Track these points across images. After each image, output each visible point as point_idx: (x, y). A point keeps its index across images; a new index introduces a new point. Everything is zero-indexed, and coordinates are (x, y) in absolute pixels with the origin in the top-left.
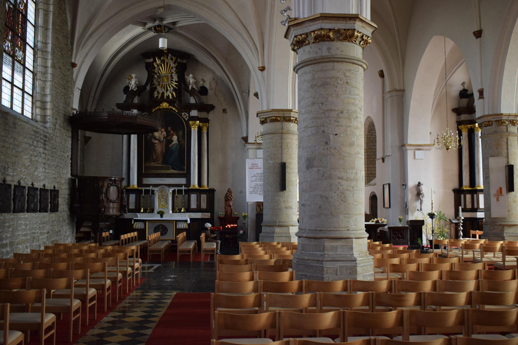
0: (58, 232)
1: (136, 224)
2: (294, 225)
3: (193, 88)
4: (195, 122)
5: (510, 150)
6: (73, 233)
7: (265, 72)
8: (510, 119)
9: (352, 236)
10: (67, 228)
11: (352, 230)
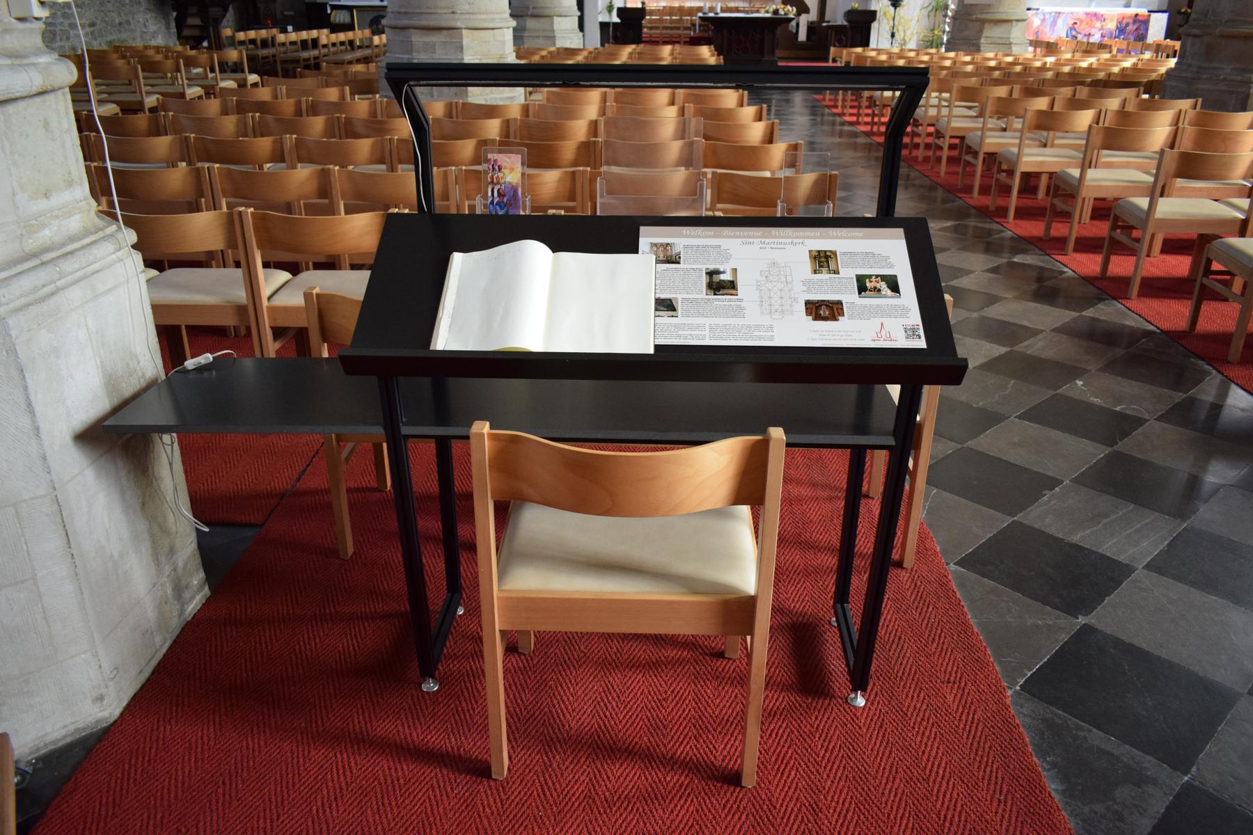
0: (120, 24)
1: (336, 14)
2: (565, 14)
6: (168, 28)
9: (459, 24)
10: (148, 16)
11: (462, 14)
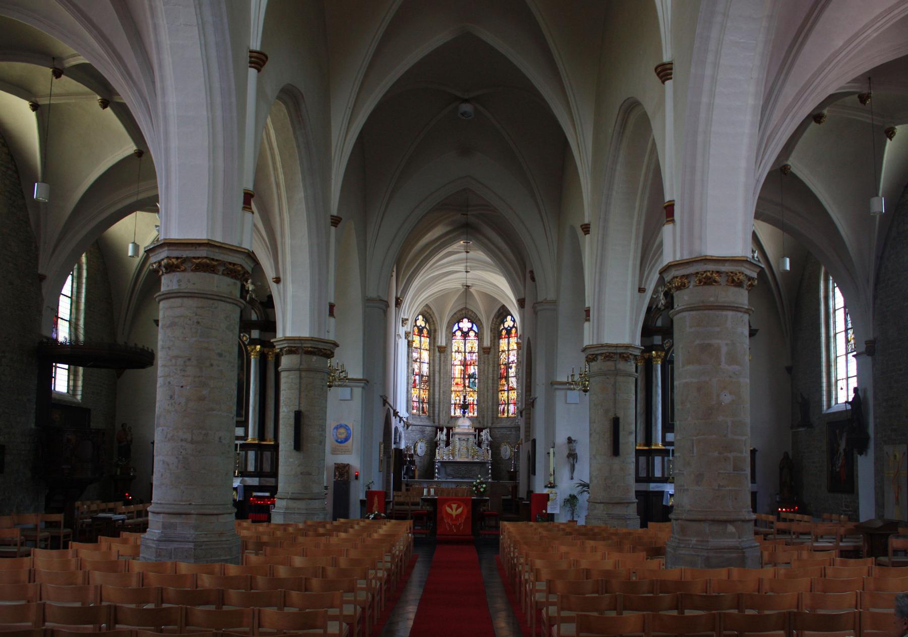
3: (251, 298)
4: (256, 347)
5: (619, 396)
7: (281, 284)
8: (618, 351)
